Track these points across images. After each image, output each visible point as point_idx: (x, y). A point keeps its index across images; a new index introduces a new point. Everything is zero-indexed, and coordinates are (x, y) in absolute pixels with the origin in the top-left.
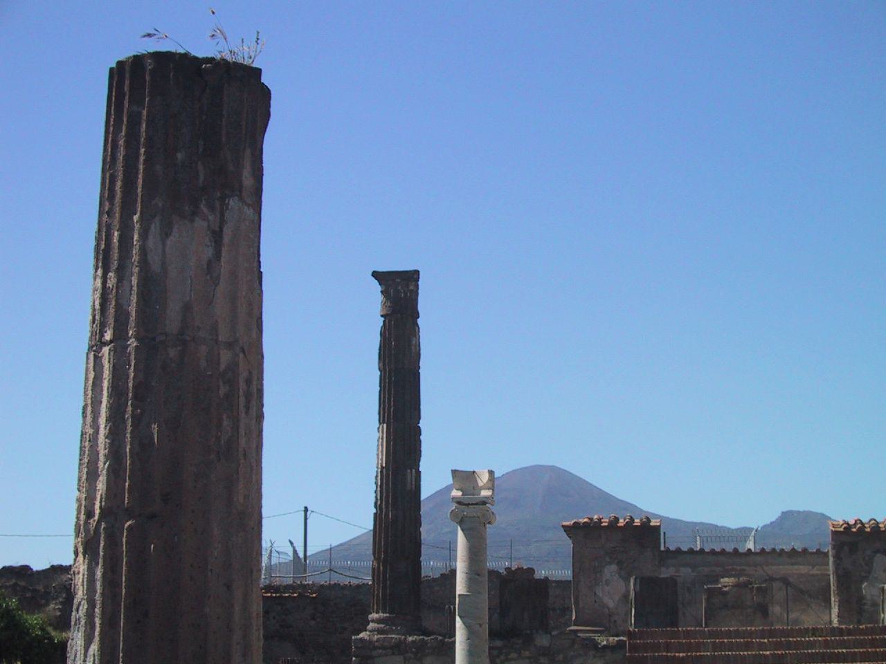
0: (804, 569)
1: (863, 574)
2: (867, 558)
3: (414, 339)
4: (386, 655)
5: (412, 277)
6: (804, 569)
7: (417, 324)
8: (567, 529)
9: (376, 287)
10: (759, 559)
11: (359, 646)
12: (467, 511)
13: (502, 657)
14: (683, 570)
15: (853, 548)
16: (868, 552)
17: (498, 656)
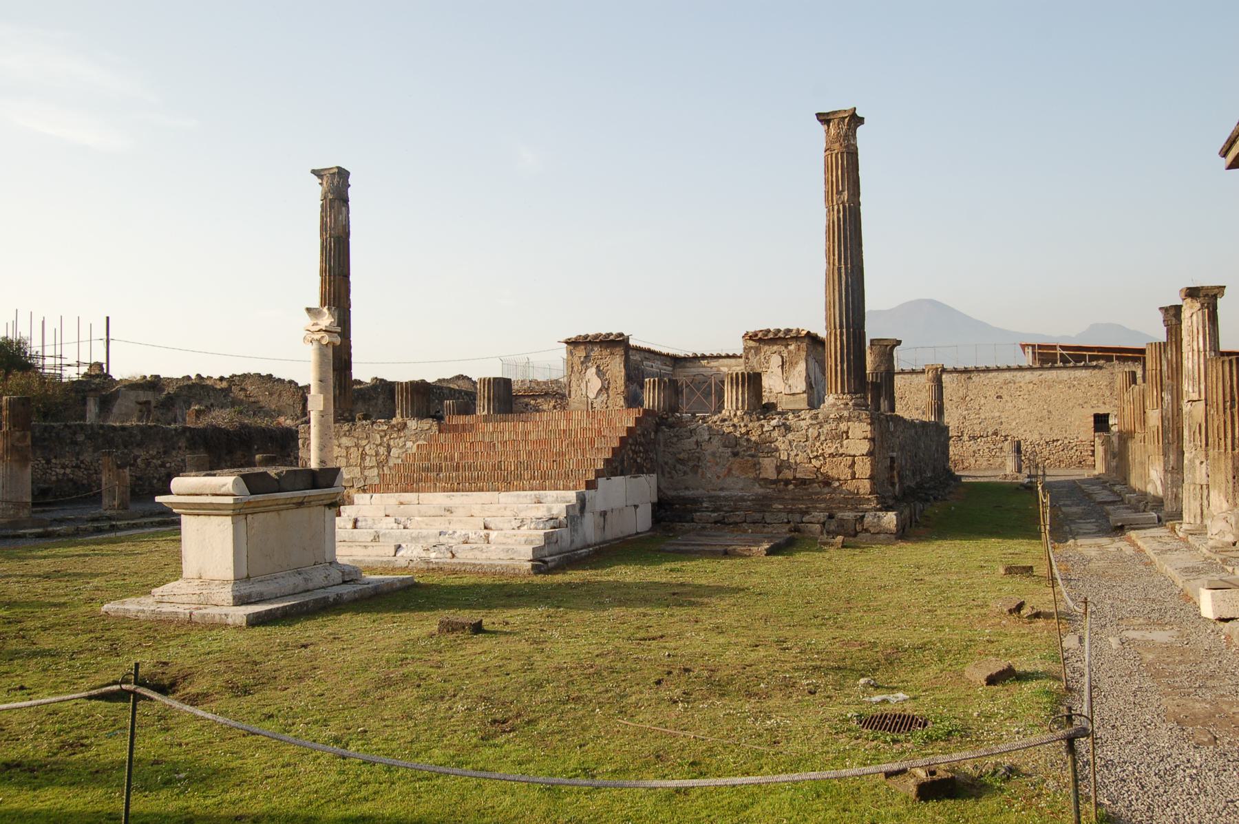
1: (764, 370)
13: (388, 437)
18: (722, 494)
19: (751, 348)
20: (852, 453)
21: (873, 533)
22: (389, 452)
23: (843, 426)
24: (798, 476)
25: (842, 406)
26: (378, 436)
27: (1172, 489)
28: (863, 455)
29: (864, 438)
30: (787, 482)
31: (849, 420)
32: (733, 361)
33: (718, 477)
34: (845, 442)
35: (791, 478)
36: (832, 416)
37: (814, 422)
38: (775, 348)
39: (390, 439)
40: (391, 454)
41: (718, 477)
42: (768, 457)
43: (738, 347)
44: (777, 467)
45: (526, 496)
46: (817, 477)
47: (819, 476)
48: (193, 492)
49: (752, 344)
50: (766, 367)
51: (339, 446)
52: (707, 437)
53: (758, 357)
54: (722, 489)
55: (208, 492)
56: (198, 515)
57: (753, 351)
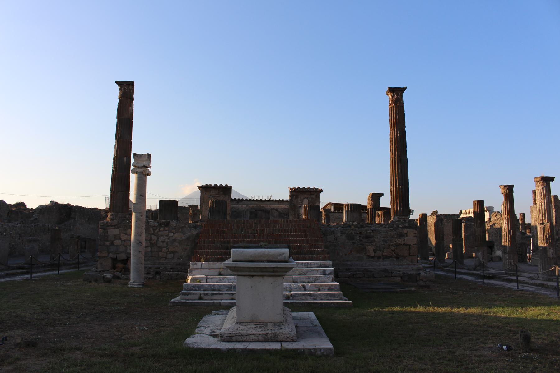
0: (283, 206)
1: (300, 206)
2: (301, 200)
3: (131, 108)
4: (112, 229)
5: (131, 84)
6: (283, 206)
7: (133, 103)
8: (199, 187)
9: (117, 87)
10: (268, 203)
11: (102, 225)
12: (138, 170)
13: (158, 230)
14: (244, 206)
15: (297, 197)
16: (302, 198)
17: (156, 230)
18: (349, 263)
19: (293, 195)
20: (409, 243)
21: (425, 281)
22: (158, 239)
23: (405, 231)
24: (384, 254)
25: (403, 221)
26: (152, 230)
27: (508, 260)
28: (414, 245)
29: (415, 237)
30: (379, 257)
31: (407, 228)
32: (249, 203)
33: (346, 255)
34: (406, 238)
35: (381, 255)
36: (400, 226)
37: (392, 229)
38: (305, 196)
39: (160, 231)
40: (159, 239)
41: (346, 255)
42: (370, 245)
43: (286, 197)
44: (374, 250)
45: (302, 264)
46: (393, 255)
47: (394, 254)
48: (251, 259)
49: (294, 193)
50: (301, 205)
51: (126, 234)
52: (339, 235)
53: (297, 200)
54: (347, 261)
55: (265, 259)
56: (253, 276)
57: (295, 197)
